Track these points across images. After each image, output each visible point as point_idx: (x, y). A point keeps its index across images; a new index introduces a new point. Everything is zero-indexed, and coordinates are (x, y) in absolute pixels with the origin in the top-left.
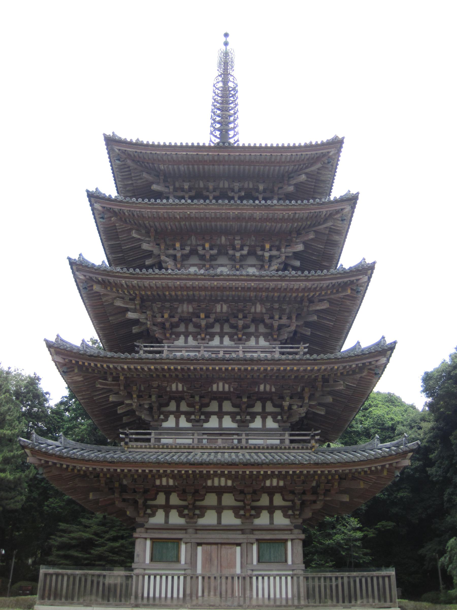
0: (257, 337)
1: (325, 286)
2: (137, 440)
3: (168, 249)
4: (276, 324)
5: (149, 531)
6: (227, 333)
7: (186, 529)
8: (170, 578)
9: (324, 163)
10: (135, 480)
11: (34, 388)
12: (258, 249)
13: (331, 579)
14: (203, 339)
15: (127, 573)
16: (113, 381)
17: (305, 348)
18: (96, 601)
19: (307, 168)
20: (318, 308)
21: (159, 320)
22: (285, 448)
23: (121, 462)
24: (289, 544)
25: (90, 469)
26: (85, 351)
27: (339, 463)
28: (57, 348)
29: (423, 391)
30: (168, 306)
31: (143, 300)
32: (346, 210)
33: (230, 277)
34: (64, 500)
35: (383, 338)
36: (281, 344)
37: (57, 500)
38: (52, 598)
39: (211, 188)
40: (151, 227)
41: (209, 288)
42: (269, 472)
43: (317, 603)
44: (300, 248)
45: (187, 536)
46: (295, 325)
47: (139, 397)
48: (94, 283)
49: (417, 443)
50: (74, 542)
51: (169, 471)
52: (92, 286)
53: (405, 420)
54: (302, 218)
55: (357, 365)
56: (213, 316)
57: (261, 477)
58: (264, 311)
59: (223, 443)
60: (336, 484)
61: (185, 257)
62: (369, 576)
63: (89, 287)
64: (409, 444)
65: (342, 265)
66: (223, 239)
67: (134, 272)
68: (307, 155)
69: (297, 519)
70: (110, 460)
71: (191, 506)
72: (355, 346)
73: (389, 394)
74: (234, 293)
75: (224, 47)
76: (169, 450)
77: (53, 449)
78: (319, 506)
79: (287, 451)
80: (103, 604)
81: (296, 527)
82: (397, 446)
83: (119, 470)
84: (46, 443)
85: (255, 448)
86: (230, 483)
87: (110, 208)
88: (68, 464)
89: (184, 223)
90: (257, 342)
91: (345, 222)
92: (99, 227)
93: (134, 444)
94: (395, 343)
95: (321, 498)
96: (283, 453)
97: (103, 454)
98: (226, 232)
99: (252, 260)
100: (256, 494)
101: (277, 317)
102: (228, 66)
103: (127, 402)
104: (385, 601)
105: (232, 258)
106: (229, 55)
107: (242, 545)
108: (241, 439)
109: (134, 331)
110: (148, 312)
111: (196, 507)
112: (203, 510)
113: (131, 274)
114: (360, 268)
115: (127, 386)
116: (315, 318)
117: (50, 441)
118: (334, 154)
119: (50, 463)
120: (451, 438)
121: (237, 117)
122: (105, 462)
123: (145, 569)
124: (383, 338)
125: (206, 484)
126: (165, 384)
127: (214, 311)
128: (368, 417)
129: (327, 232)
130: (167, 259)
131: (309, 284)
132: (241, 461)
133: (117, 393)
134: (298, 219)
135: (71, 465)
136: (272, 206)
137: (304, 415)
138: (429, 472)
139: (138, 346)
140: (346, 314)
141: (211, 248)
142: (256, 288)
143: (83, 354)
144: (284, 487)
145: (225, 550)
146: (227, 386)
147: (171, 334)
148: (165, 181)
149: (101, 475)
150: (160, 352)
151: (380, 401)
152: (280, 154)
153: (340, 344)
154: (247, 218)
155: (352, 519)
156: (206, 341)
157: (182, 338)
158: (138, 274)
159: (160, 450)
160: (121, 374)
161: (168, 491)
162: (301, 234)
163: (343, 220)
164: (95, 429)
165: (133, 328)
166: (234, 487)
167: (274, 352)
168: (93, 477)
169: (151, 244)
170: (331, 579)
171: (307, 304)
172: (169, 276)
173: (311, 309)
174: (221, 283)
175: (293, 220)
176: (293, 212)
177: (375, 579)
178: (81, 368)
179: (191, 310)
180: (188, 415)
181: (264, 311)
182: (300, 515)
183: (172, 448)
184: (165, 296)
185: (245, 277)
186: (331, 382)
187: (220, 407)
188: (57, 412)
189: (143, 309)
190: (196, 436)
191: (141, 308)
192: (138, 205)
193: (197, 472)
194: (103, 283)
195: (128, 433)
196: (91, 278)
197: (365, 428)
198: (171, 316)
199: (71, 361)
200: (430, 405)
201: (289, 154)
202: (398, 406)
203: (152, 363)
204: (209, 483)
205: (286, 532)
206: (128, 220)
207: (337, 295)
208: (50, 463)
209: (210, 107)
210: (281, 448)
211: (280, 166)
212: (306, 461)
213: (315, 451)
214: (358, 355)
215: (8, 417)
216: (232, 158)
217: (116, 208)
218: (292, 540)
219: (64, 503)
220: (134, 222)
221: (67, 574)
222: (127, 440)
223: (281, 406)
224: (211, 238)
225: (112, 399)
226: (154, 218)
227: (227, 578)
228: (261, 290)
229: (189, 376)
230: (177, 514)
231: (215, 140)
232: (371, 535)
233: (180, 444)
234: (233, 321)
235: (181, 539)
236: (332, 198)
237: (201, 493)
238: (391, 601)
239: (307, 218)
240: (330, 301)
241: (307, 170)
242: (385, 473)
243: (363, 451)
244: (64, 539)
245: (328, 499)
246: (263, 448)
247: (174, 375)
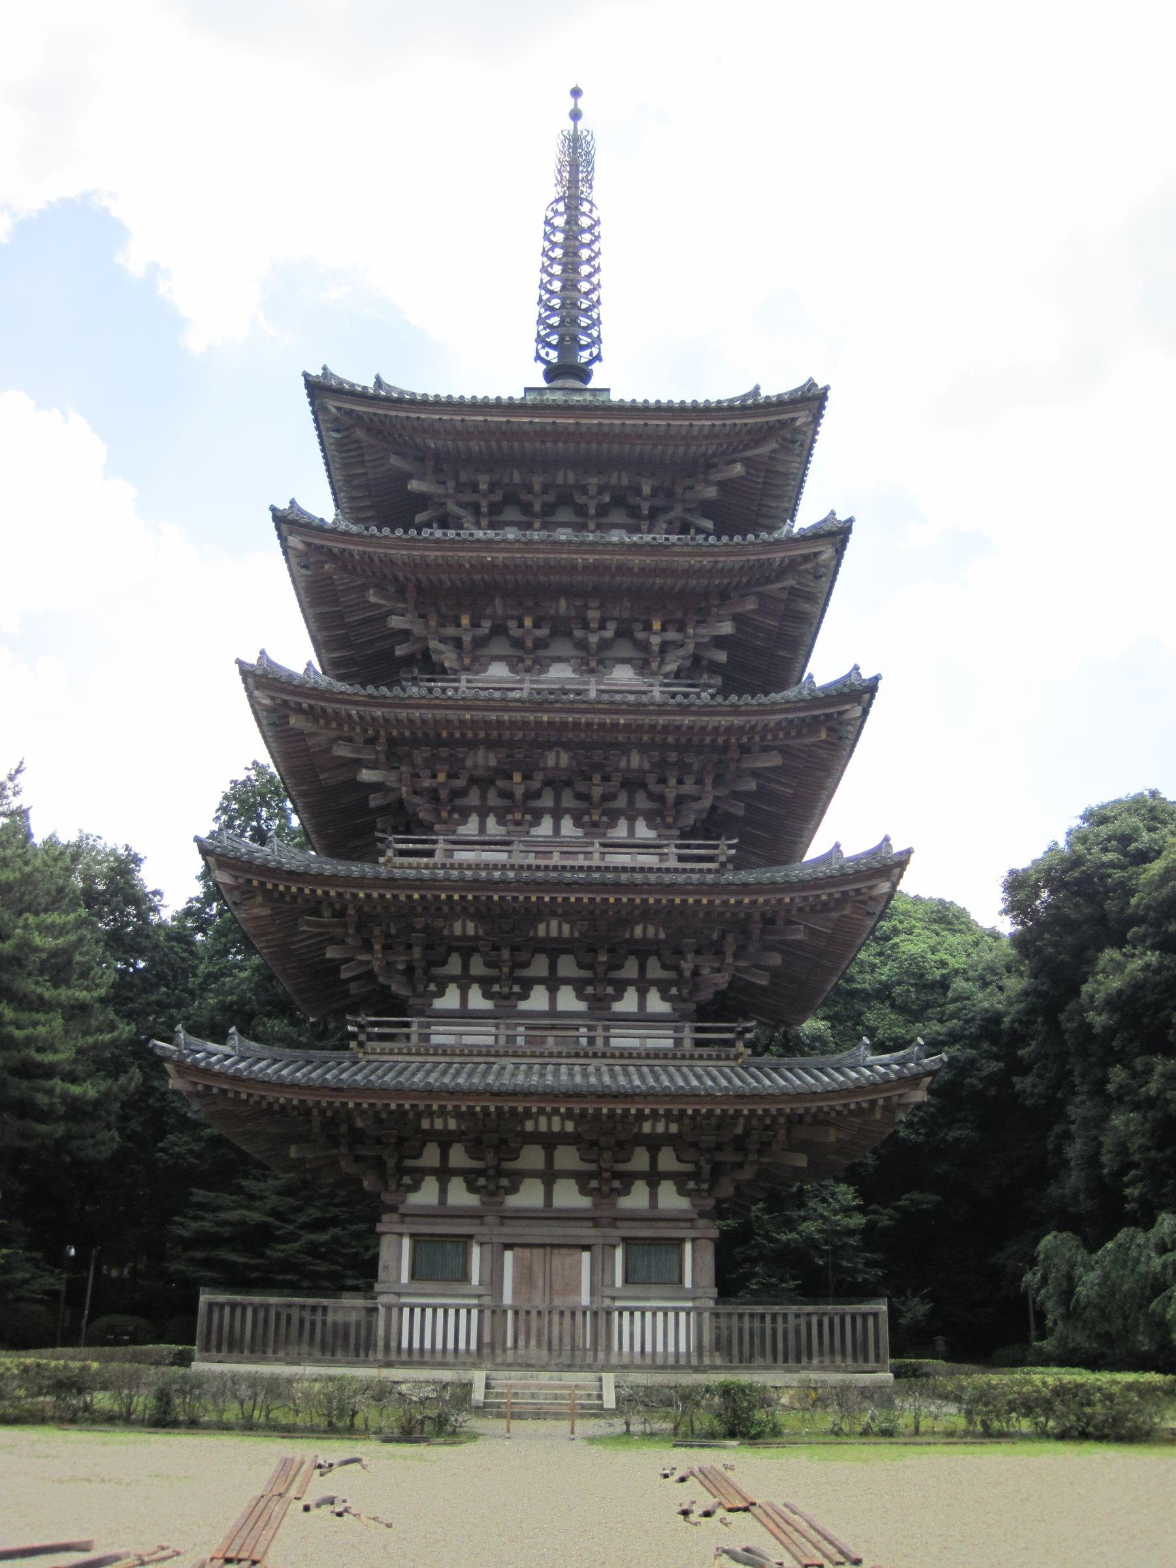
0: (632, 820)
1: (772, 724)
2: (382, 1037)
3: (444, 626)
4: (671, 794)
5: (407, 1219)
6: (568, 811)
7: (481, 1217)
8: (451, 1312)
9: (784, 439)
10: (379, 1121)
11: (127, 882)
12: (638, 626)
13: (763, 1316)
14: (518, 823)
15: (369, 1303)
16: (334, 916)
17: (730, 847)
18: (310, 1354)
19: (746, 447)
20: (759, 764)
21: (427, 783)
22: (683, 1057)
23: (356, 1089)
24: (688, 1247)
25: (295, 1102)
26: (280, 862)
27: (784, 1094)
28: (222, 855)
29: (1005, 912)
30: (445, 755)
31: (391, 742)
32: (824, 557)
33: (575, 706)
34: (201, 1139)
35: (887, 839)
36: (683, 836)
37: (186, 1138)
38: (225, 1348)
39: (537, 488)
40: (408, 580)
41: (532, 725)
42: (647, 1111)
43: (735, 1363)
44: (727, 628)
46: (711, 797)
47: (387, 947)
48: (289, 712)
49: (941, 1059)
50: (226, 1231)
51: (450, 1108)
52: (287, 716)
53: (971, 966)
54: (731, 570)
55: (830, 895)
56: (539, 777)
57: (632, 1119)
58: (647, 766)
59: (557, 1044)
60: (782, 1132)
61: (480, 642)
62: (836, 1314)
63: (280, 718)
64: (926, 1061)
65: (810, 677)
66: (563, 604)
67: (376, 693)
68: (746, 424)
69: (703, 1198)
70: (333, 1084)
71: (491, 1172)
72: (830, 853)
73: (941, 902)
74: (583, 736)
75: (570, 125)
76: (448, 1059)
77: (219, 1061)
78: (747, 1174)
79: (687, 1062)
80: (324, 1361)
81: (702, 1214)
82: (902, 1063)
83: (351, 1105)
84: (204, 1050)
85: (622, 1056)
86: (570, 1127)
87: (323, 547)
88: (250, 1091)
89: (479, 577)
90: (631, 831)
91: (824, 579)
92: (297, 579)
93: (377, 1046)
94: (909, 852)
95: (753, 1157)
96: (678, 1068)
97: (319, 1071)
98: (568, 592)
99: (623, 649)
100: (623, 1148)
101: (673, 782)
102: (577, 172)
103: (363, 957)
104: (866, 1360)
105: (582, 645)
106: (581, 146)
107: (594, 1248)
108: (594, 1037)
109: (372, 804)
110: (403, 769)
111: (501, 1173)
112: (516, 1180)
113: (370, 696)
114: (846, 690)
116: (752, 785)
117: (211, 1046)
118: (806, 424)
119: (215, 1091)
120: (1062, 1017)
121: (598, 302)
122: (324, 1088)
124: (887, 839)
125: (523, 1128)
126: (439, 923)
127: (542, 765)
128: (889, 956)
129: (784, 596)
130: (442, 647)
131: (737, 721)
132: (592, 1090)
133: (341, 942)
134: (722, 570)
135: (258, 1093)
136: (667, 547)
137: (725, 986)
138: (1018, 1087)
139: (382, 840)
140: (819, 773)
141: (537, 625)
142: (630, 725)
143: (274, 870)
144: (679, 1135)
145: (559, 1260)
146: (566, 928)
147: (450, 813)
148: (438, 470)
149: (315, 1112)
150: (430, 854)
151: (921, 919)
152: (687, 423)
153: (811, 826)
154: (613, 568)
155: (843, 1187)
158: (384, 697)
159: (430, 1059)
160: (350, 906)
161: (445, 1141)
162: (729, 598)
163: (818, 577)
164: (271, 978)
165: (371, 796)
167: (667, 854)
168: (296, 1113)
169: (409, 616)
170: (763, 1316)
171: (737, 755)
172: (450, 703)
173: (744, 765)
174: (557, 717)
175: (711, 572)
176: (712, 559)
177: (848, 1320)
178: (267, 894)
179: (493, 762)
180: (485, 984)
181: (647, 766)
182: (710, 1191)
183: (453, 1054)
184: (439, 735)
185: (607, 706)
186: (780, 924)
187: (553, 967)
188: (180, 936)
190: (503, 1031)
191: (387, 758)
192: (382, 541)
193: (506, 1108)
194: (311, 713)
195: (363, 1022)
196: (285, 702)
197: (880, 982)
198: (452, 776)
199: (249, 881)
200: (1018, 941)
201: (708, 423)
202: (960, 931)
203: (416, 888)
205: (682, 1224)
206: (359, 568)
207: (799, 741)
208: (215, 1091)
209: (535, 311)
210: (674, 1057)
211: (688, 447)
212: (720, 1090)
213: (743, 1063)
214: (832, 877)
215: (78, 958)
216: (584, 429)
217: (336, 546)
218: (694, 1240)
219: (202, 1144)
220: (374, 573)
221: (251, 1304)
222: (362, 1037)
223: (677, 968)
224: (537, 604)
225: (331, 953)
226: (416, 565)
227: (562, 1313)
228: (640, 727)
229: (489, 909)
230: (464, 1185)
231: (547, 354)
232: (885, 1222)
233: (471, 1046)
234: (581, 787)
235: (471, 1237)
236: (795, 530)
237: (513, 1145)
238: (877, 1360)
239: (742, 568)
240: (783, 751)
241: (749, 453)
242: (878, 1115)
243: (838, 1070)
244: (207, 1224)
245: (766, 1160)
246: (639, 1057)
247: (458, 908)
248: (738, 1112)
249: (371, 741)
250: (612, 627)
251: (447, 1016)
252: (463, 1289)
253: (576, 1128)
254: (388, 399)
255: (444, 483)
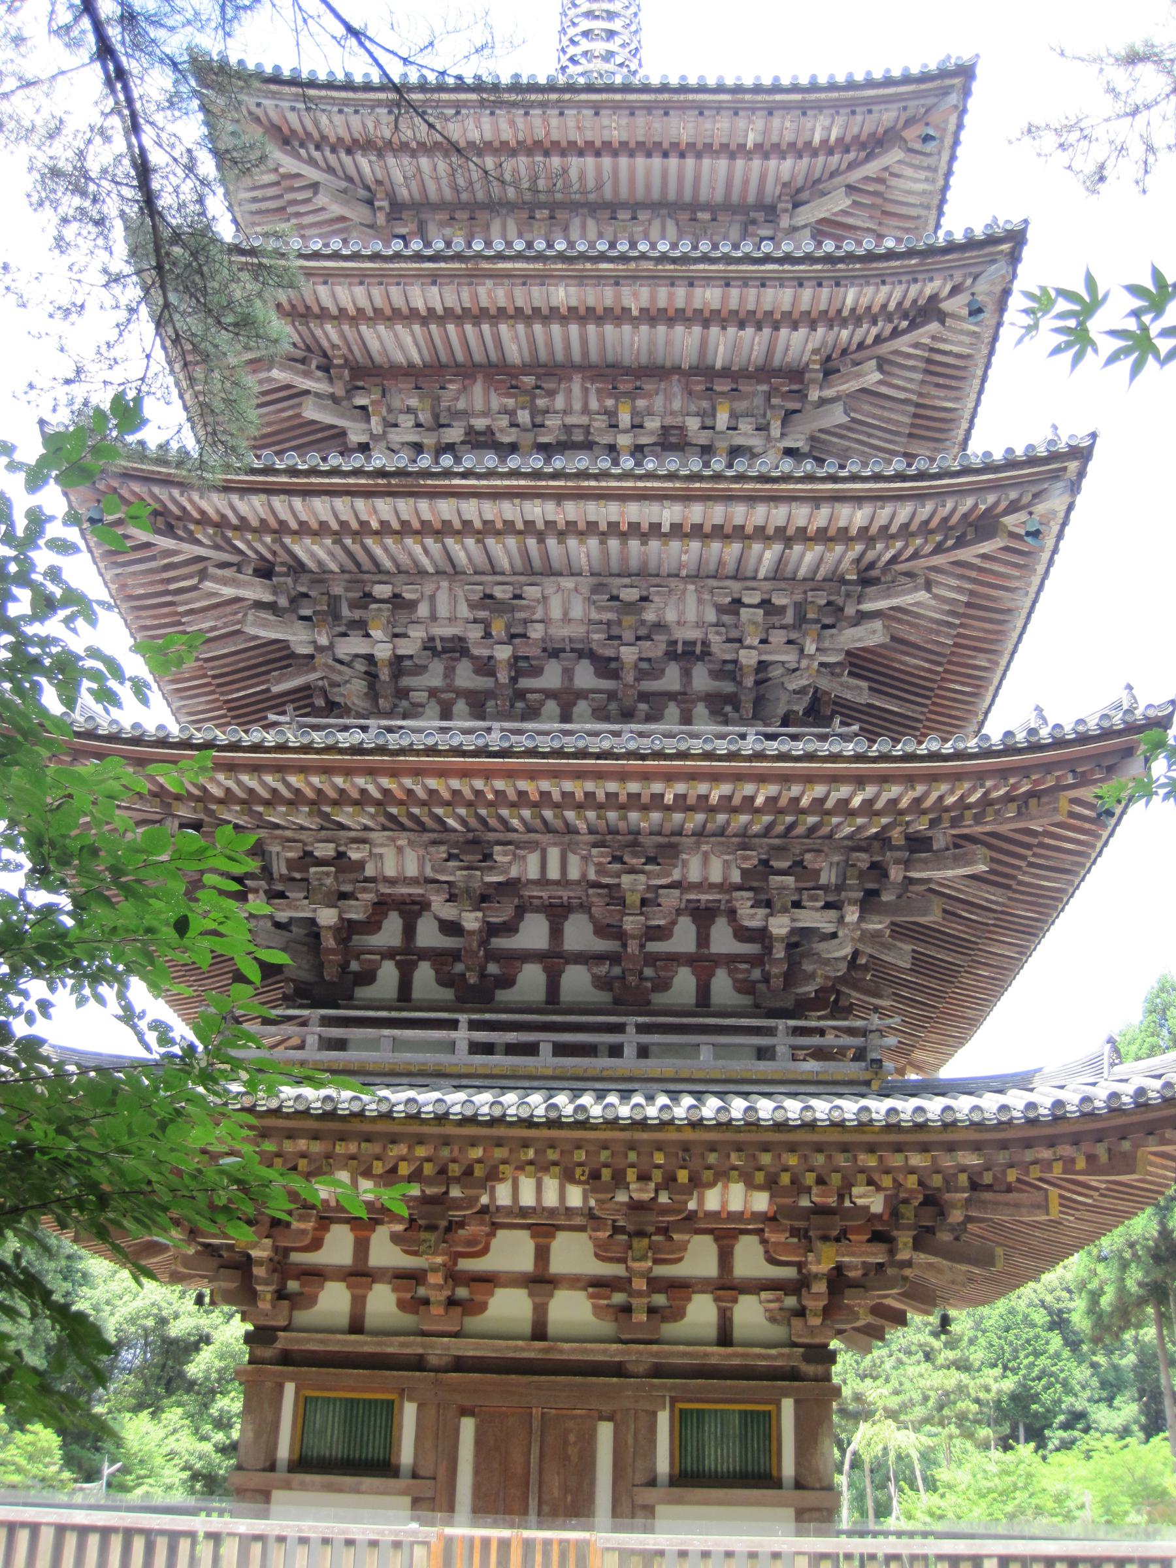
86: (575, 1197)
146: (574, 861)
166: (591, 1209)
204: (503, 1195)
236: (941, 239)
241: (855, 176)
253: (585, 1199)
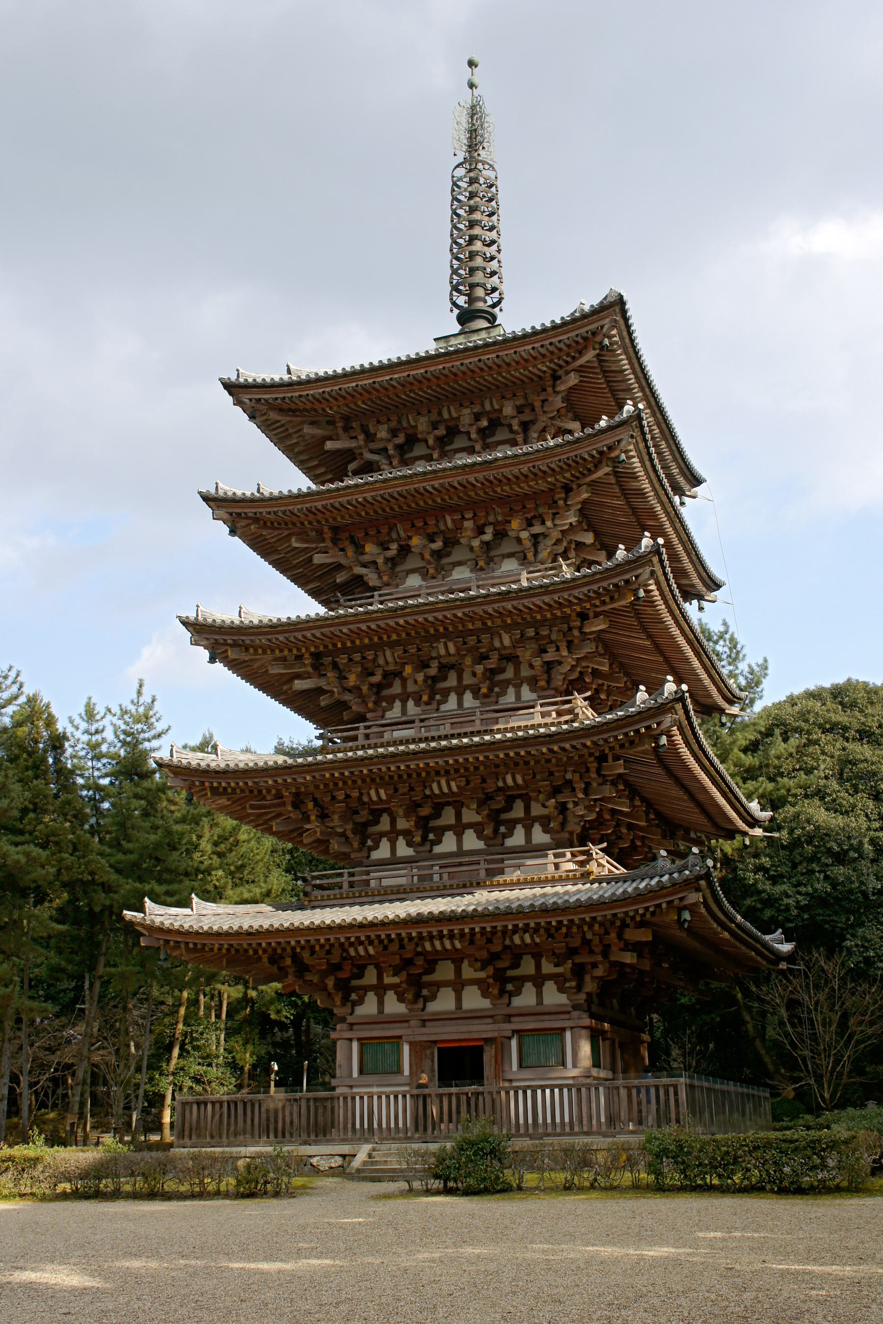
2: (321, 887)
24: (568, 1035)
45: (409, 1031)
52: (226, 651)
61: (393, 562)
66: (448, 519)
81: (576, 1007)
109: (323, 704)
115: (297, 804)
117: (174, 910)
123: (351, 1087)
150: (355, 738)
156: (434, 705)
157: (398, 704)
177: (653, 1091)
189: (318, 668)
217: (250, 511)
235: (400, 1037)
248: (560, 923)
249: (299, 658)
250: (489, 530)
251: (382, 863)
252: (398, 1079)
254: (300, 383)
255: (355, 437)
